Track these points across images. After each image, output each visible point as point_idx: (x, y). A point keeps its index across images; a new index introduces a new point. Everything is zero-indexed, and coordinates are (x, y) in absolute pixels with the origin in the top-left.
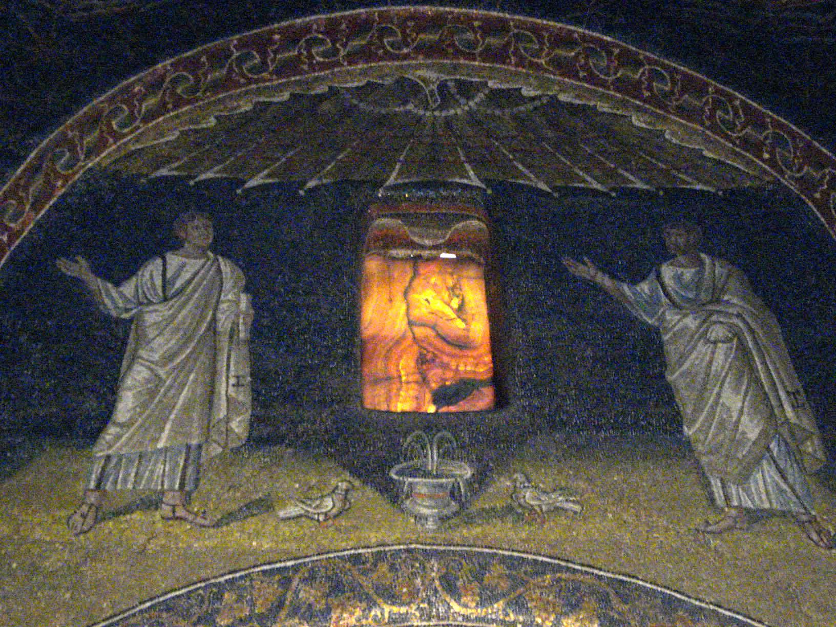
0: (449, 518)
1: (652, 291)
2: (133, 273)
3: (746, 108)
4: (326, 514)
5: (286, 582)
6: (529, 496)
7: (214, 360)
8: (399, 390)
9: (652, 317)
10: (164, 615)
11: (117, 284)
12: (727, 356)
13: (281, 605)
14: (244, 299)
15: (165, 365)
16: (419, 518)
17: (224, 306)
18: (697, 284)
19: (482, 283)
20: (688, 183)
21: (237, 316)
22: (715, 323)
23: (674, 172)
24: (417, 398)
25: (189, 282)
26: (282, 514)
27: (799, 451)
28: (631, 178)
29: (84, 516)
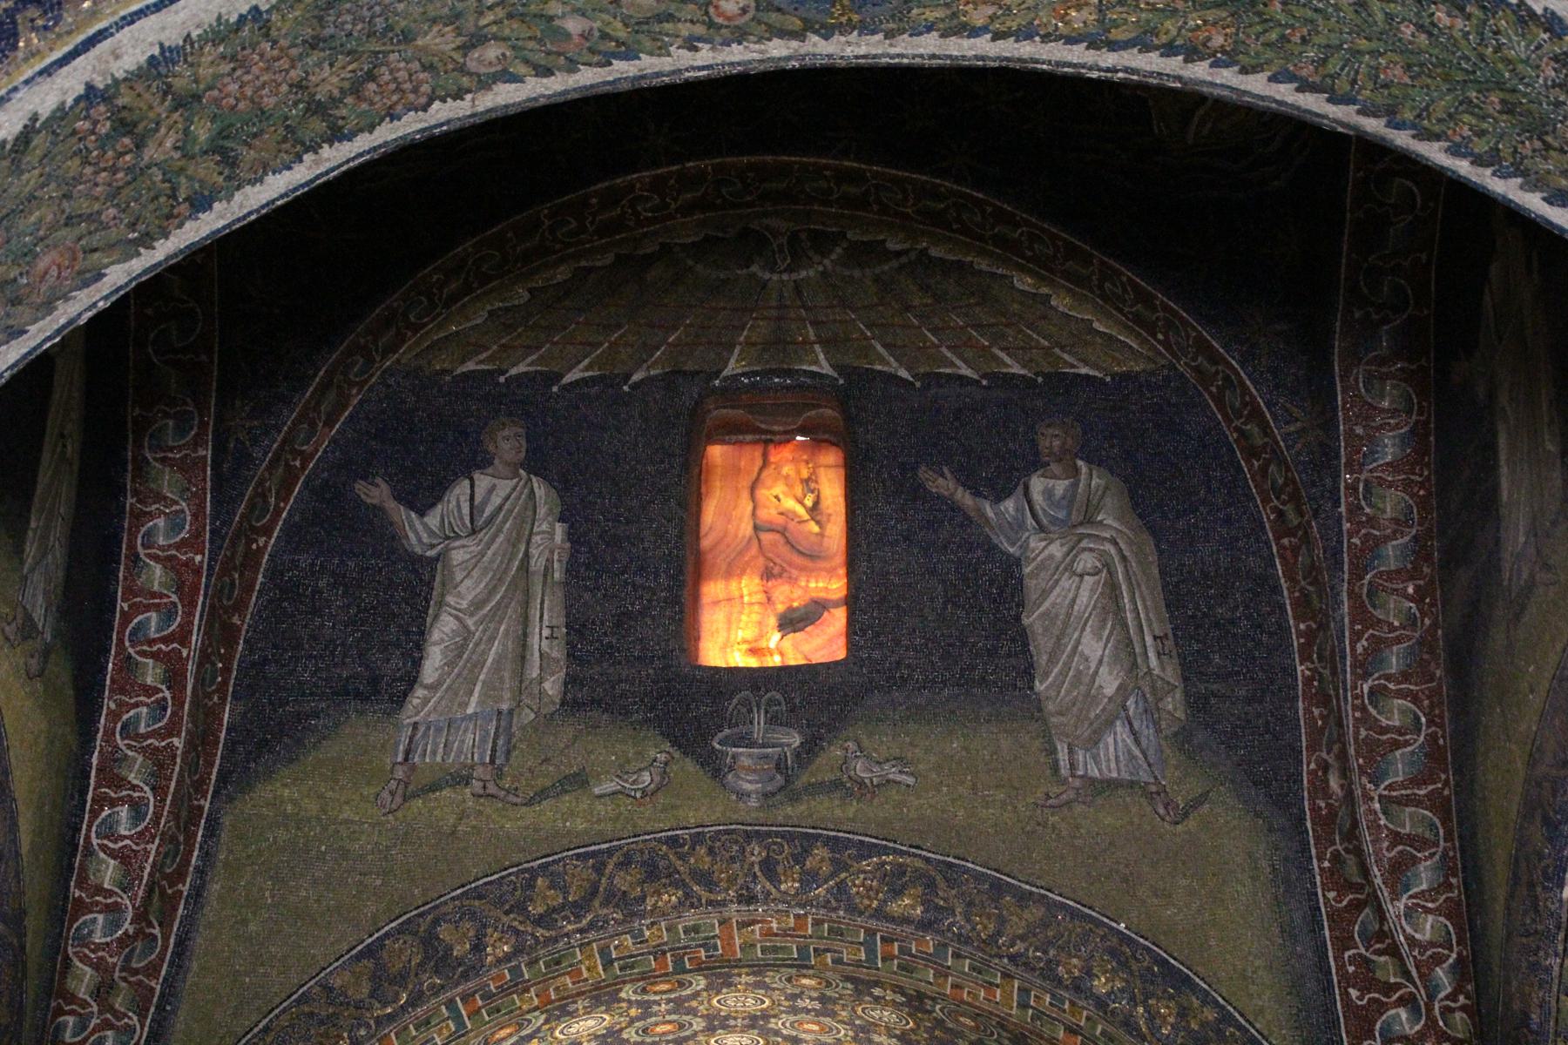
0: (773, 794)
1: (1017, 510)
2: (439, 499)
3: (1135, 286)
4: (643, 790)
5: (599, 869)
6: (860, 768)
7: (526, 604)
8: (741, 613)
9: (1013, 544)
10: (477, 903)
11: (422, 514)
12: (1093, 591)
13: (594, 892)
14: (560, 529)
15: (472, 615)
16: (742, 795)
17: (537, 539)
18: (1070, 498)
19: (842, 472)
20: (1073, 366)
21: (552, 552)
22: (1084, 549)
23: (1057, 350)
24: (760, 623)
25: (500, 508)
26: (597, 791)
27: (1158, 709)
28: (1007, 360)
29: (392, 793)
